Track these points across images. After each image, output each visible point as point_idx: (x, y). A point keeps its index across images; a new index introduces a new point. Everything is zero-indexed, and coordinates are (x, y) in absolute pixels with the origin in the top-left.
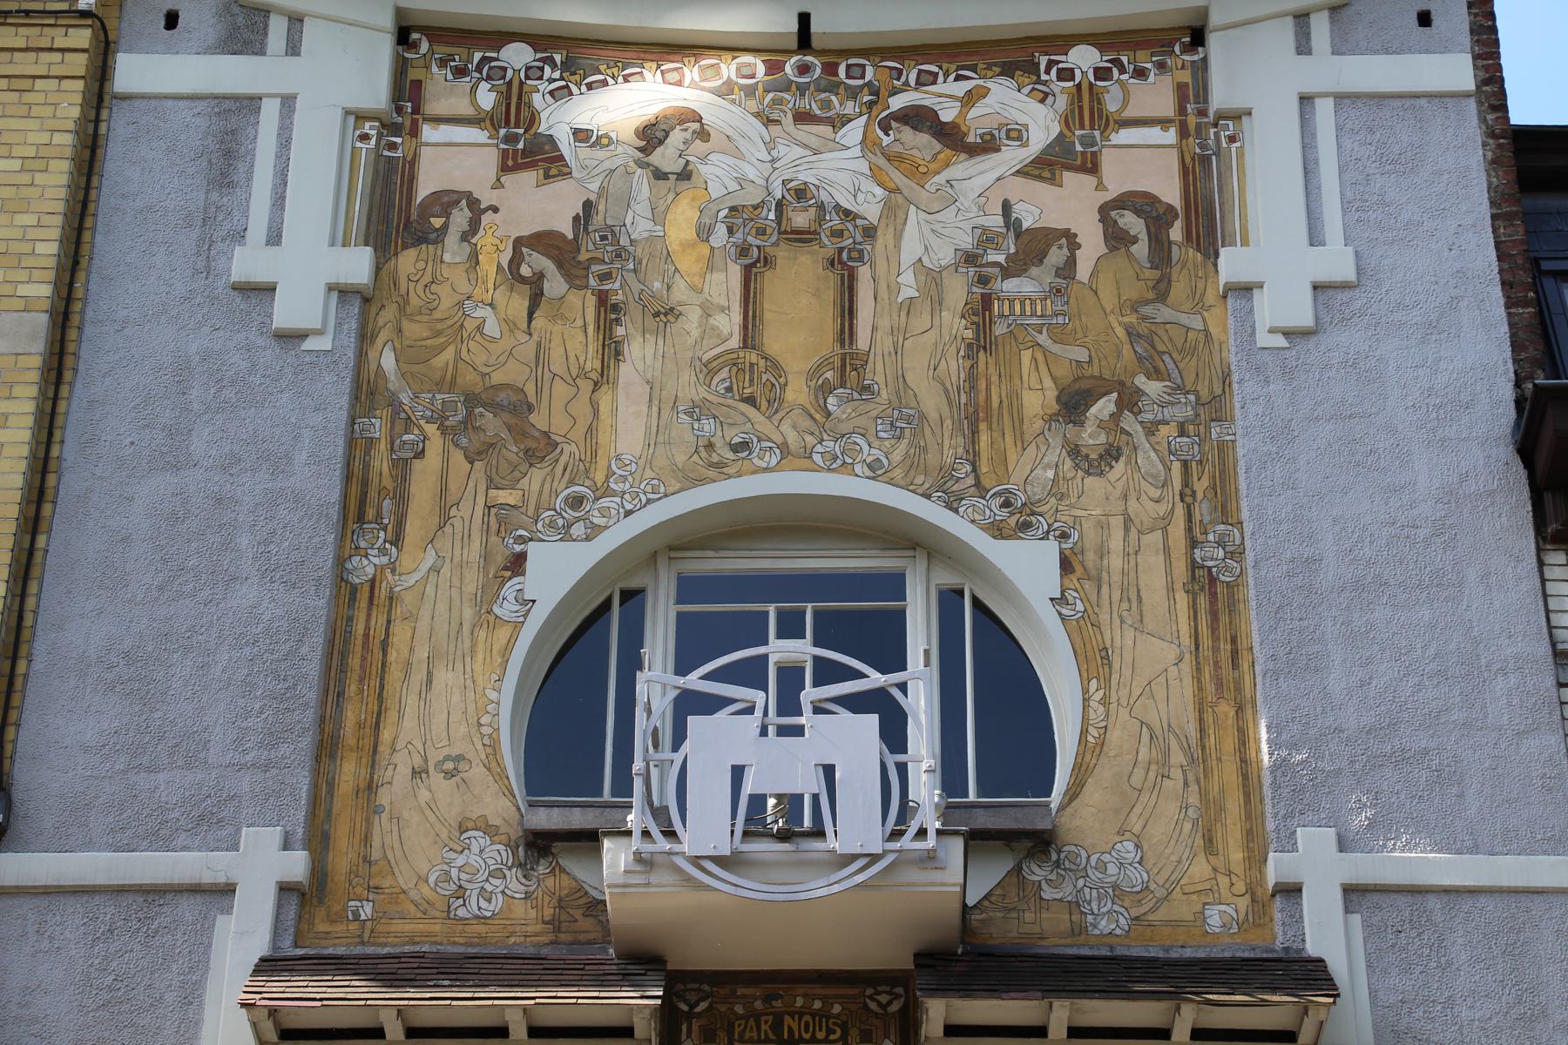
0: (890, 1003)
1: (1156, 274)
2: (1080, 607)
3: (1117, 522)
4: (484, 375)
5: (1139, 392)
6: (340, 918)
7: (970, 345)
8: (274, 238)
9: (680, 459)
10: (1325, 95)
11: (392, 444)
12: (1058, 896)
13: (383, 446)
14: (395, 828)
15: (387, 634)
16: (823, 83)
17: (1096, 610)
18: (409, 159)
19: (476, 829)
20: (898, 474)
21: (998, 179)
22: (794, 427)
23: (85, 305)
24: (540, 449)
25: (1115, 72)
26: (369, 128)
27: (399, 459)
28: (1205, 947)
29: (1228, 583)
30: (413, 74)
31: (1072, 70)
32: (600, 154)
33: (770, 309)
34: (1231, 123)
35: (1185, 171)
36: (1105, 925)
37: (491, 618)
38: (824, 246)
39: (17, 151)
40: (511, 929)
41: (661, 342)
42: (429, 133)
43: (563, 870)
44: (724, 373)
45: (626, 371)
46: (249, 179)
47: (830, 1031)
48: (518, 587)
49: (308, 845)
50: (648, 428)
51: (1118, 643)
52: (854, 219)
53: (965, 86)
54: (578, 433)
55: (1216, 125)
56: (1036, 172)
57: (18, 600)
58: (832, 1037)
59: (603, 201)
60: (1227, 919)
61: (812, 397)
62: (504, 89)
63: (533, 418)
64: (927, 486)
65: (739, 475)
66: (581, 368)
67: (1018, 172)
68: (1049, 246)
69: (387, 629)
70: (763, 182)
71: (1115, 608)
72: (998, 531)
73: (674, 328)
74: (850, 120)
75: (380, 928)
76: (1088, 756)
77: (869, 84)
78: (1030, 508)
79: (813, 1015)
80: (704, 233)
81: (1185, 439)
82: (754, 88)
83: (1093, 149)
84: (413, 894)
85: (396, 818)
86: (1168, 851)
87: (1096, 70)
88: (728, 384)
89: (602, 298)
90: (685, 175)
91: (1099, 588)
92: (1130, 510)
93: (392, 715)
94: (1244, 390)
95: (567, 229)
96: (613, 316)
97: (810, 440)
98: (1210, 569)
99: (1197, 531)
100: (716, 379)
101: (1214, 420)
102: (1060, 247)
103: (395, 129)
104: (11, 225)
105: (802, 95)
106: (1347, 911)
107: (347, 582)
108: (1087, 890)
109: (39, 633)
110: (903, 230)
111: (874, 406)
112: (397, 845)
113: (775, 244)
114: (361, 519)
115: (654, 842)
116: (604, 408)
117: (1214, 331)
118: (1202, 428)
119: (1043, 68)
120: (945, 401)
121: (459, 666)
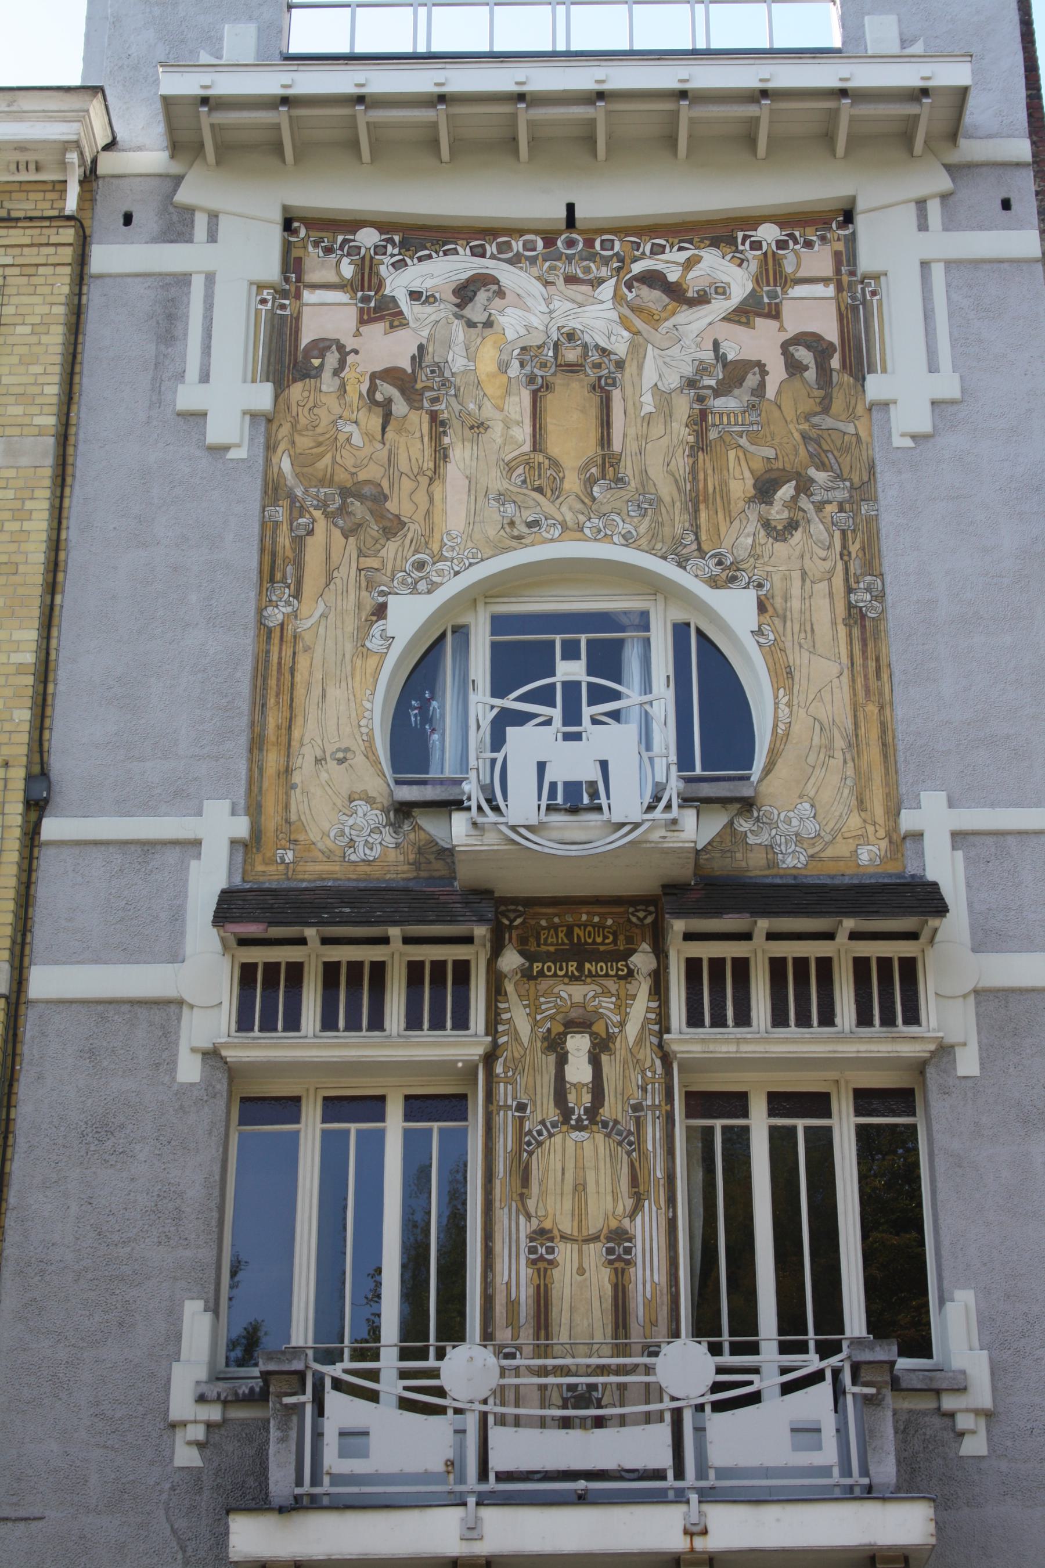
0: (645, 917)
1: (822, 393)
2: (772, 637)
3: (796, 575)
4: (353, 474)
5: (812, 481)
6: (272, 861)
7: (692, 447)
8: (205, 377)
9: (492, 532)
10: (938, 261)
11: (291, 525)
12: (758, 842)
13: (285, 527)
14: (306, 799)
15: (294, 662)
16: (584, 254)
17: (783, 639)
18: (295, 315)
19: (360, 799)
20: (643, 542)
21: (710, 324)
22: (570, 509)
23: (78, 429)
24: (394, 526)
25: (791, 243)
26: (266, 294)
27: (297, 536)
28: (857, 875)
29: (873, 618)
30: (296, 253)
31: (760, 242)
32: (428, 309)
33: (552, 424)
34: (872, 282)
35: (841, 317)
36: (790, 862)
37: (365, 650)
38: (588, 375)
39: (29, 320)
40: (387, 868)
41: (475, 448)
42: (308, 296)
43: (420, 828)
44: (520, 470)
45: (453, 471)
46: (186, 335)
47: (605, 937)
48: (382, 628)
49: (248, 812)
50: (468, 511)
51: (798, 662)
52: (608, 355)
53: (686, 254)
54: (419, 516)
55: (862, 282)
56: (737, 318)
57: (45, 641)
58: (607, 941)
59: (431, 344)
60: (873, 856)
61: (583, 487)
62: (359, 262)
63: (388, 505)
64: (664, 550)
65: (533, 544)
66: (420, 468)
67: (724, 318)
68: (747, 373)
69: (294, 658)
70: (542, 328)
71: (796, 637)
72: (714, 583)
73: (483, 438)
74: (604, 281)
75: (299, 868)
76: (778, 742)
77: (617, 254)
78: (736, 566)
79: (594, 927)
80: (503, 367)
81: (844, 514)
82: (536, 258)
83: (777, 301)
84: (320, 845)
85: (306, 792)
86: (833, 809)
87: (778, 242)
88: (522, 478)
89: (434, 416)
90: (489, 324)
91: (785, 623)
92: (806, 567)
93: (299, 721)
94: (885, 476)
95: (406, 365)
96: (441, 429)
97: (582, 518)
98: (861, 608)
99: (852, 580)
100: (514, 475)
101: (862, 500)
102: (754, 374)
103: (285, 294)
104: (27, 374)
105: (570, 263)
106: (954, 848)
107: (265, 625)
108: (778, 837)
109: (61, 664)
110: (643, 362)
111: (626, 493)
112: (307, 811)
113: (554, 374)
114: (272, 580)
115: (487, 816)
116: (437, 497)
117: (863, 434)
118: (855, 506)
119: (740, 240)
120: (675, 488)
121: (344, 684)
